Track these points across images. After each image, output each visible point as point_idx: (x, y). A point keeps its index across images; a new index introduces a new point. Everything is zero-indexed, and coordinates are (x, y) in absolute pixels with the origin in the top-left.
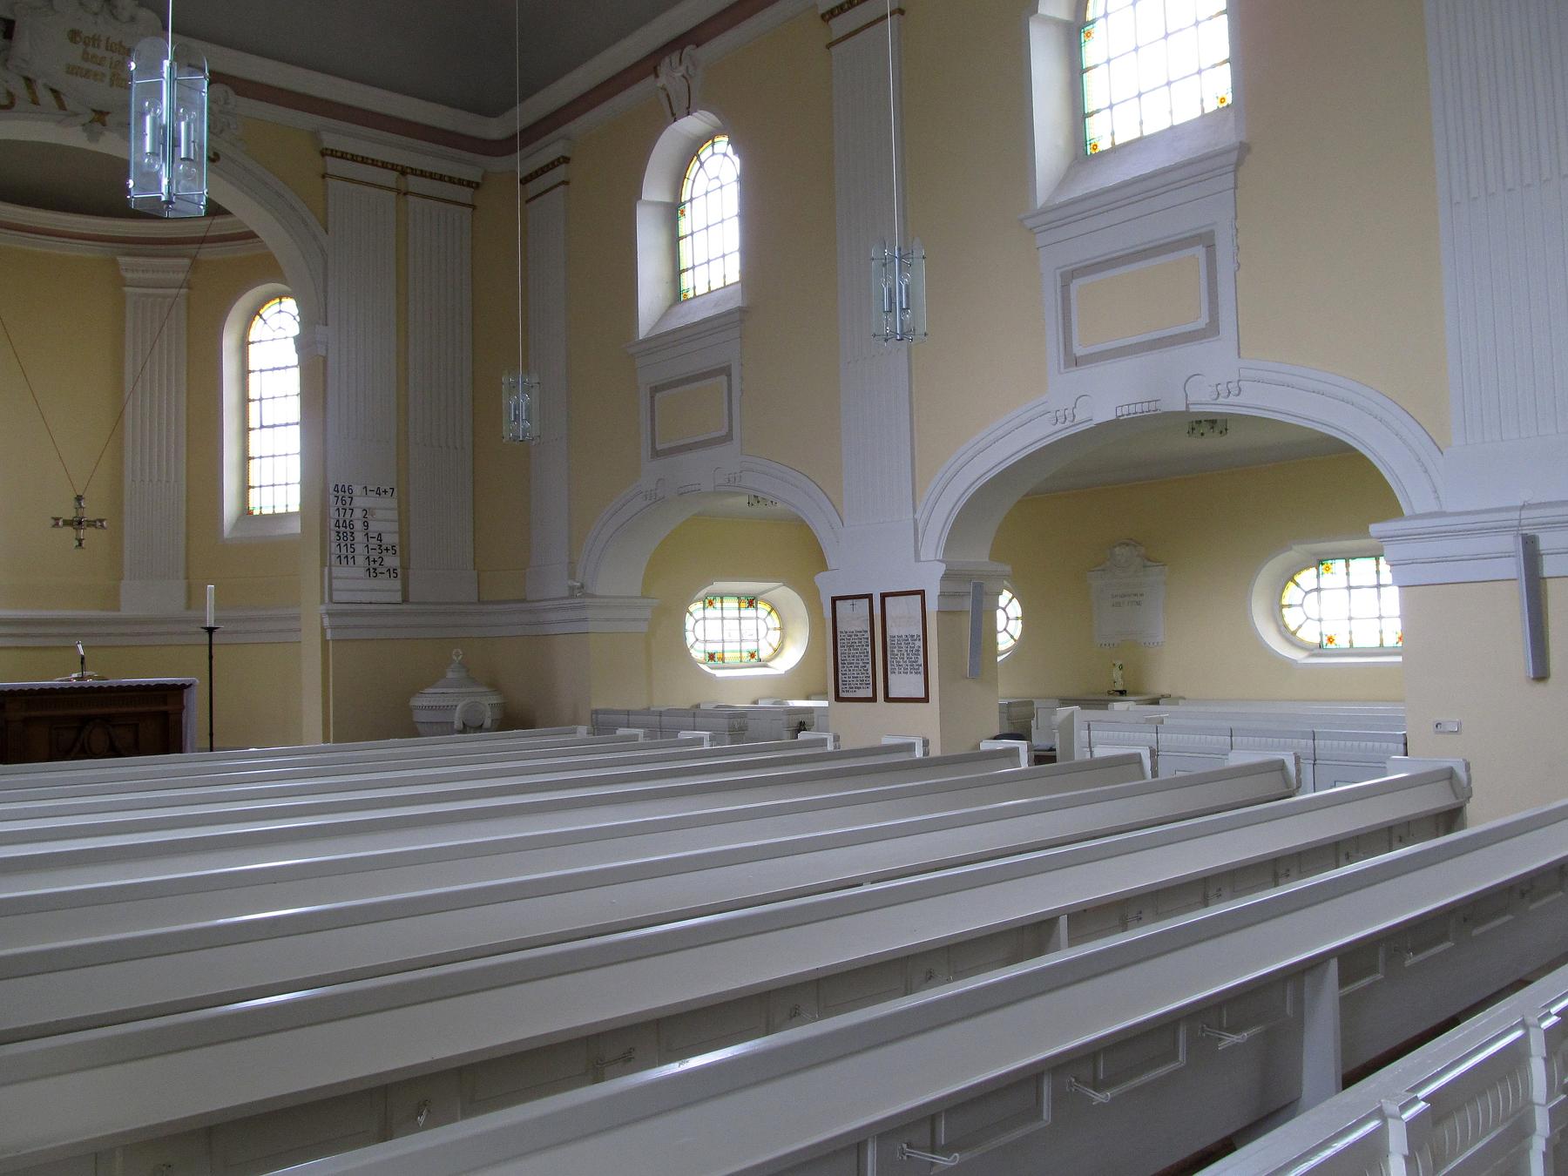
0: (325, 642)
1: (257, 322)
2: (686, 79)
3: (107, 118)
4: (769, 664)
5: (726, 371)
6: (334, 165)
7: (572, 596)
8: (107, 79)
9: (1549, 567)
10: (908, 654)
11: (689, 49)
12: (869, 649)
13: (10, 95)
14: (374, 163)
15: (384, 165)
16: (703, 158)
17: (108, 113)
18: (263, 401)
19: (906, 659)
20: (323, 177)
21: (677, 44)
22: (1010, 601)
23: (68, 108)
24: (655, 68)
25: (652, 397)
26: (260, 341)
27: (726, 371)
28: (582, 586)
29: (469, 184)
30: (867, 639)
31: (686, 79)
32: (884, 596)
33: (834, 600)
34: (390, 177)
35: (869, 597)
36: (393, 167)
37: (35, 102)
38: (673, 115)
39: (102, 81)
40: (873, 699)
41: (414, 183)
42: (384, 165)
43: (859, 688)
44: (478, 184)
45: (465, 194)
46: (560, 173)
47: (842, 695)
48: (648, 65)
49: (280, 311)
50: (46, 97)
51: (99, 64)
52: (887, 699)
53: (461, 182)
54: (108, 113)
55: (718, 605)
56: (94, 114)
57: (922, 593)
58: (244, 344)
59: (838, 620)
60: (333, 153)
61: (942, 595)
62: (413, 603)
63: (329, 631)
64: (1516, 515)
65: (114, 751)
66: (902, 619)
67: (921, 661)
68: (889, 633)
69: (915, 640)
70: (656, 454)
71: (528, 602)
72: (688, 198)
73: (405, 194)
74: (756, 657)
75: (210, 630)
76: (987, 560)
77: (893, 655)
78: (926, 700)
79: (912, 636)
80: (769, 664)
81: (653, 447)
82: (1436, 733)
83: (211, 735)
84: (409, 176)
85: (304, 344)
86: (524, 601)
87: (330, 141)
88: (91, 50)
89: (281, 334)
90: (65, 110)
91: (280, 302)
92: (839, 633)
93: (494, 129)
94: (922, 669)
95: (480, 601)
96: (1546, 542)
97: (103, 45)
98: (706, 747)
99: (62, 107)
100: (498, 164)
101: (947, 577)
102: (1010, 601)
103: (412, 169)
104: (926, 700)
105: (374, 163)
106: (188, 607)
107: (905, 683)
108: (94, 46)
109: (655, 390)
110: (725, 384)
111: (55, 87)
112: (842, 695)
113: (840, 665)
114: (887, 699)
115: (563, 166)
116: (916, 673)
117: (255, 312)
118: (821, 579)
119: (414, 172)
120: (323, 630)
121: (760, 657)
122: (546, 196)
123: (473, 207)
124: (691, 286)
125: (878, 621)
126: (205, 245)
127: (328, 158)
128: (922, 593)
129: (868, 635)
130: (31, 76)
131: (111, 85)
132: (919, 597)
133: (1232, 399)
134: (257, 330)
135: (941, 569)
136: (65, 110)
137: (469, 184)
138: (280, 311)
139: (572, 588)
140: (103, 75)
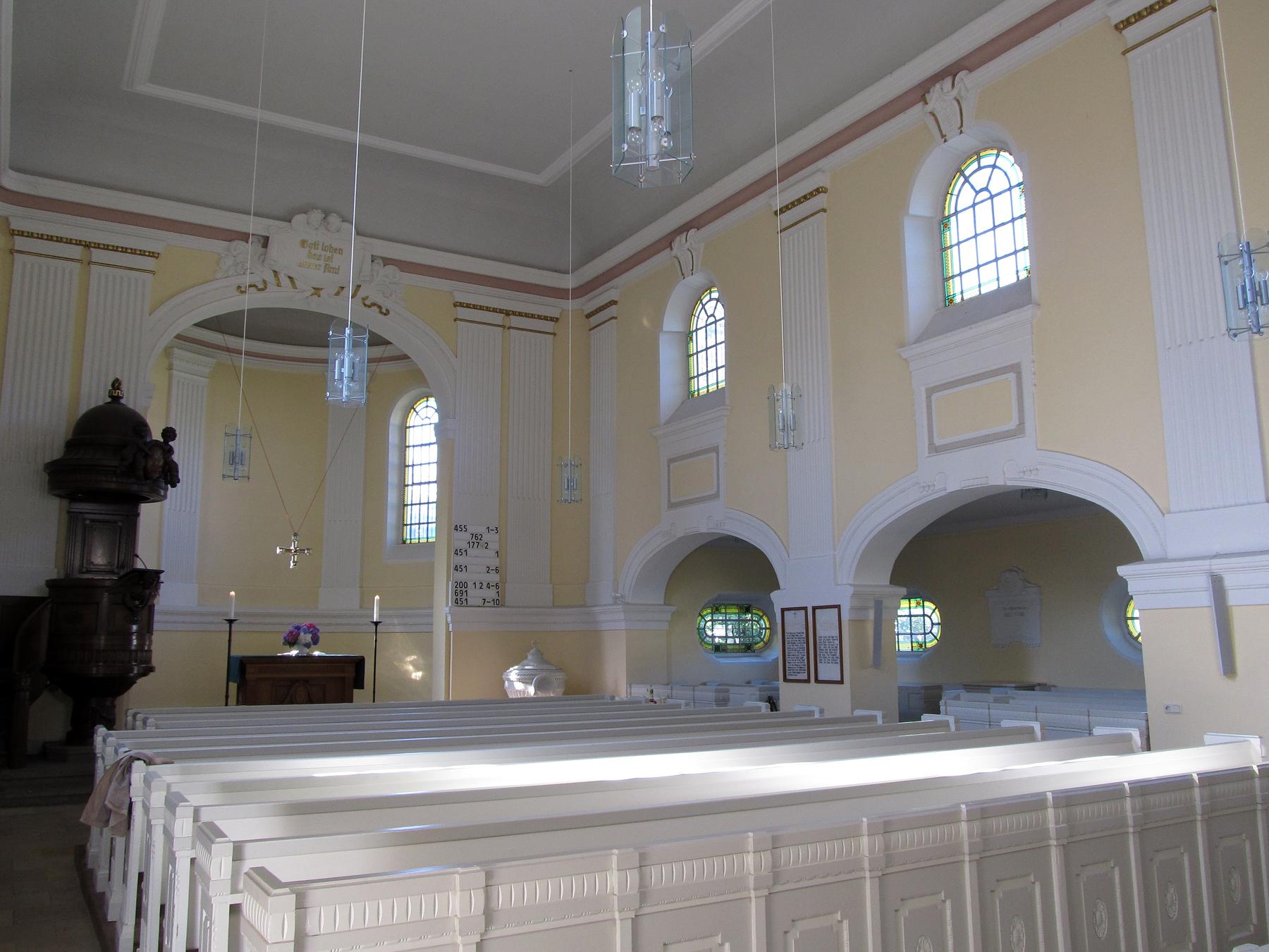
0: (448, 633)
1: (412, 414)
2: (690, 251)
3: (321, 292)
5: (716, 449)
6: (463, 313)
7: (615, 603)
8: (322, 268)
9: (1233, 599)
11: (692, 232)
12: (805, 645)
13: (265, 282)
14: (488, 309)
15: (495, 310)
16: (704, 302)
17: (322, 289)
18: (415, 467)
20: (455, 320)
21: (684, 228)
22: (934, 610)
23: (298, 287)
24: (671, 243)
25: (669, 466)
26: (414, 426)
27: (716, 449)
28: (622, 596)
29: (552, 319)
31: (690, 251)
32: (814, 609)
34: (498, 319)
35: (805, 609)
36: (501, 311)
37: (279, 285)
38: (683, 274)
39: (319, 269)
40: (808, 681)
41: (514, 321)
42: (495, 310)
44: (557, 319)
45: (548, 326)
46: (613, 310)
47: (788, 677)
48: (667, 242)
49: (427, 406)
50: (285, 282)
51: (318, 259)
53: (546, 318)
54: (322, 289)
55: (723, 611)
56: (313, 290)
57: (838, 607)
58: (404, 428)
60: (461, 305)
61: (852, 608)
62: (508, 607)
63: (451, 625)
65: (310, 700)
66: (826, 625)
67: (838, 655)
68: (818, 635)
70: (672, 506)
71: (588, 607)
72: (694, 329)
73: (509, 328)
75: (376, 624)
76: (888, 583)
78: (841, 682)
79: (833, 637)
81: (669, 501)
82: (1167, 713)
83: (374, 692)
84: (511, 316)
85: (440, 429)
86: (584, 606)
87: (461, 298)
88: (313, 251)
89: (427, 421)
90: (296, 288)
91: (427, 401)
92: (786, 635)
93: (569, 282)
94: (839, 661)
95: (554, 606)
96: (1229, 581)
97: (320, 247)
98: (683, 708)
99: (294, 286)
100: (570, 304)
101: (855, 595)
102: (934, 610)
103: (513, 312)
104: (841, 682)
105: (488, 309)
106: (361, 607)
107: (828, 670)
108: (315, 248)
109: (671, 461)
110: (715, 459)
111: (291, 276)
112: (788, 677)
113: (787, 656)
114: (817, 681)
115: (614, 306)
116: (836, 663)
117: (411, 407)
118: (774, 595)
119: (514, 313)
120: (447, 625)
122: (603, 326)
123: (554, 334)
124: (696, 389)
125: (811, 626)
126: (381, 363)
127: (458, 308)
128: (838, 607)
129: (804, 635)
130: (277, 270)
131: (325, 271)
132: (837, 609)
134: (413, 419)
135: (851, 590)
136: (296, 288)
137: (552, 319)
138: (427, 406)
139: (616, 598)
140: (320, 265)
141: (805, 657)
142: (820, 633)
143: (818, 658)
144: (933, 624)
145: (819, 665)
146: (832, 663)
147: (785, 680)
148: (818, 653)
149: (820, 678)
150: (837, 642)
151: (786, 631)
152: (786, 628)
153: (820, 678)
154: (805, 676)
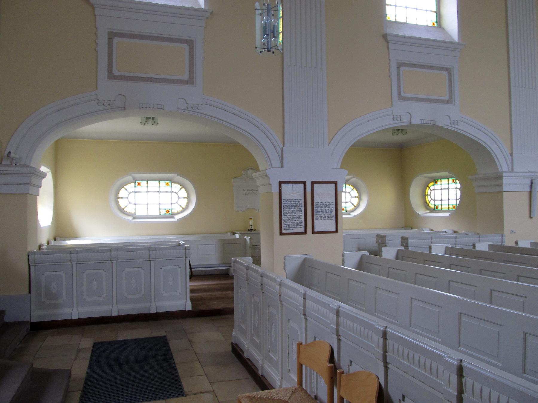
4: (350, 213)
10: (326, 211)
12: (303, 209)
19: (325, 213)
30: (301, 203)
32: (313, 183)
33: (280, 183)
35: (304, 183)
43: (295, 228)
47: (284, 231)
52: (314, 232)
59: (282, 193)
64: (533, 174)
67: (334, 213)
68: (315, 201)
69: (330, 204)
74: (345, 210)
77: (318, 211)
79: (329, 203)
80: (350, 213)
92: (282, 200)
94: (334, 218)
112: (284, 231)
113: (283, 216)
114: (314, 232)
121: (347, 210)
129: (302, 201)
133: (456, 126)
141: (303, 218)
142: (317, 199)
143: (315, 217)
144: (430, 195)
145: (315, 221)
146: (328, 220)
147: (281, 234)
148: (315, 213)
149: (316, 230)
150: (334, 206)
151: (283, 198)
152: (282, 196)
153: (316, 230)
154: (302, 230)
